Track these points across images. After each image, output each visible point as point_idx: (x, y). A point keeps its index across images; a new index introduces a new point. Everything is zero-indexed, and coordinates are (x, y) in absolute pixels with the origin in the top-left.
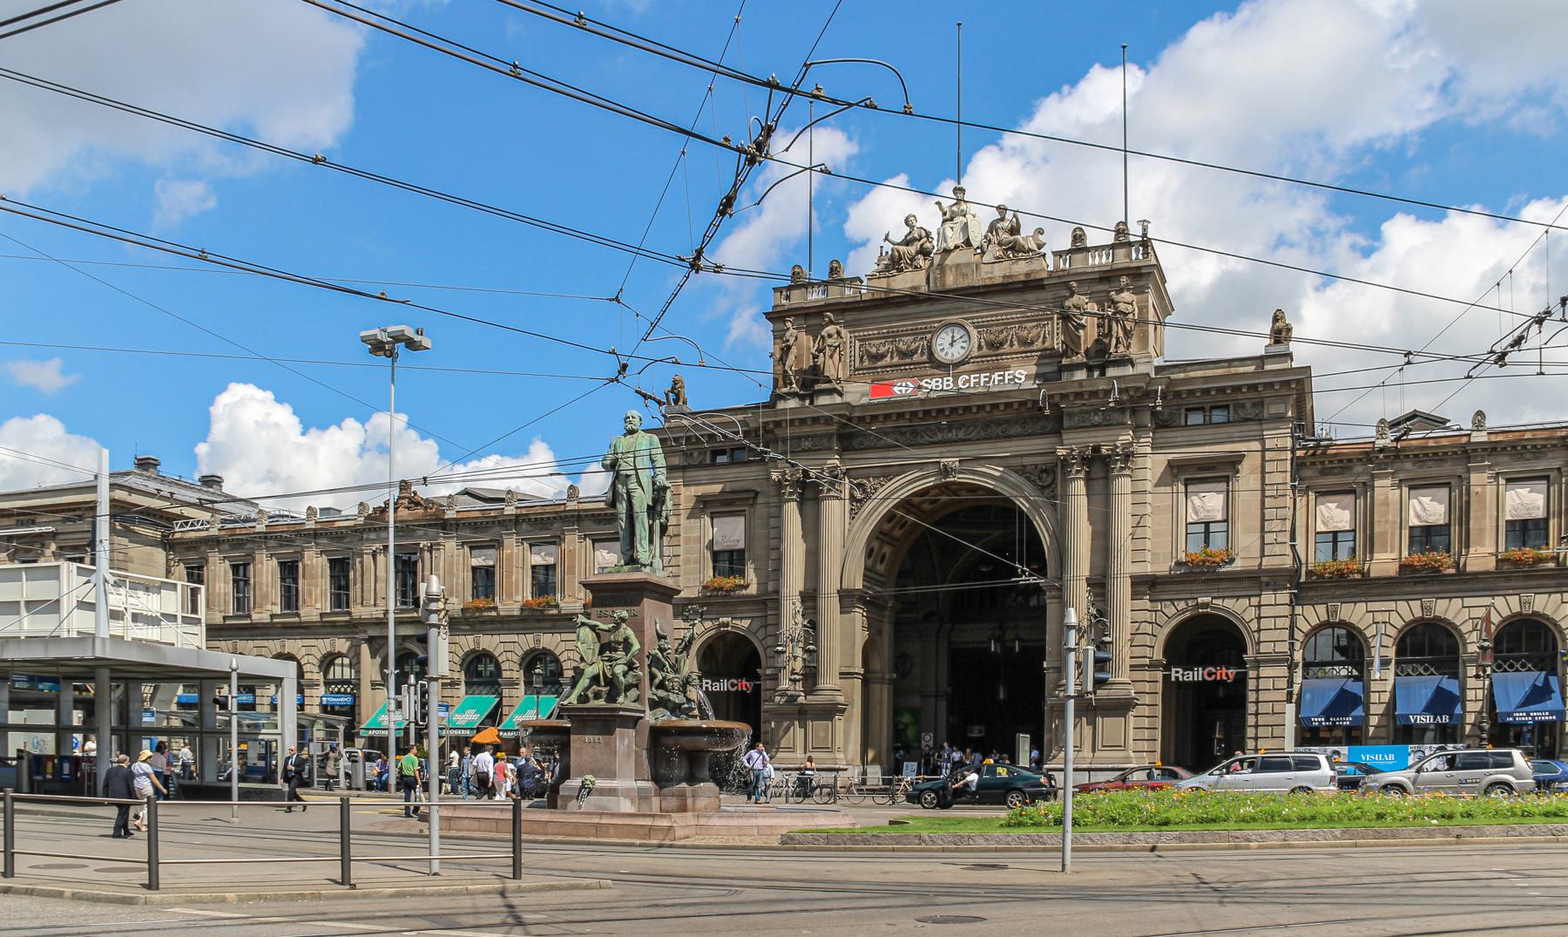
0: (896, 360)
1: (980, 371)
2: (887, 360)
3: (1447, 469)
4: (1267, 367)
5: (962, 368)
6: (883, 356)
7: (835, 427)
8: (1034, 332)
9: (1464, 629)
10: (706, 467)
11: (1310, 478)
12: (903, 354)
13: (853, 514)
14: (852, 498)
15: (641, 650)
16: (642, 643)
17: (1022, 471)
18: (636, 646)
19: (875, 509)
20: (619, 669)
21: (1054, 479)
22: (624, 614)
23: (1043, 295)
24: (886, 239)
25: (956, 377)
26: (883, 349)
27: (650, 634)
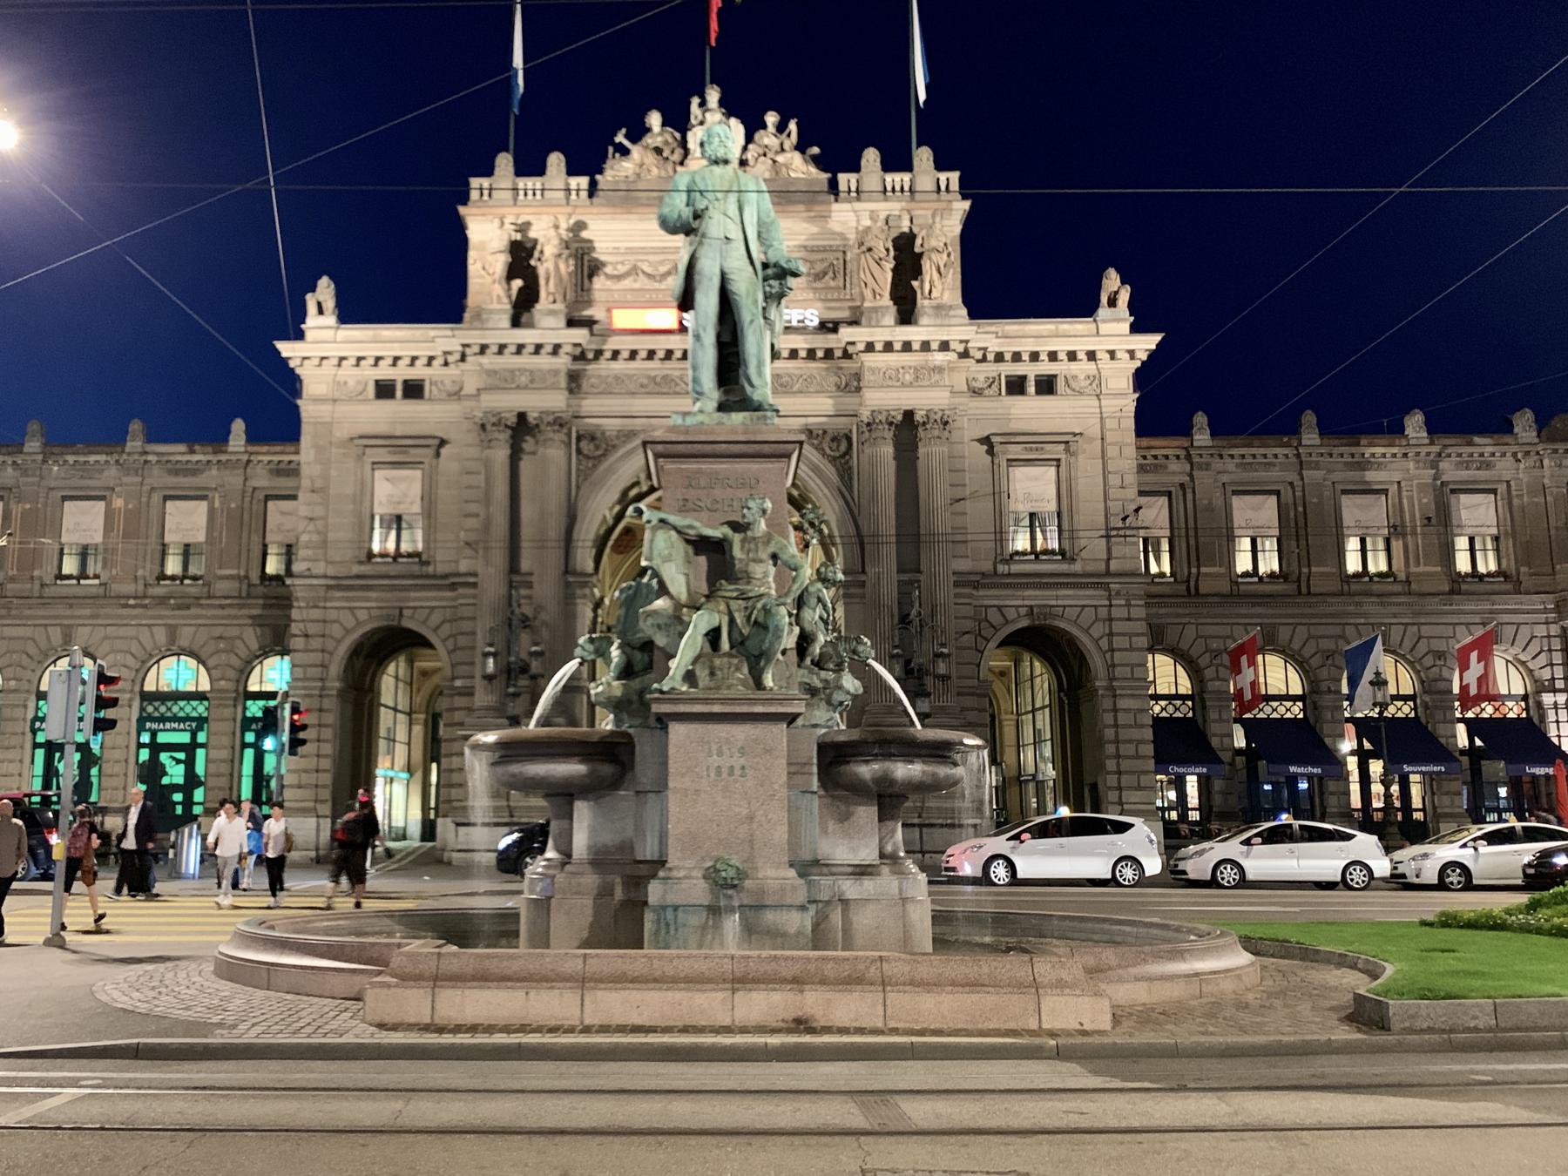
0: (637, 286)
12: (649, 276)
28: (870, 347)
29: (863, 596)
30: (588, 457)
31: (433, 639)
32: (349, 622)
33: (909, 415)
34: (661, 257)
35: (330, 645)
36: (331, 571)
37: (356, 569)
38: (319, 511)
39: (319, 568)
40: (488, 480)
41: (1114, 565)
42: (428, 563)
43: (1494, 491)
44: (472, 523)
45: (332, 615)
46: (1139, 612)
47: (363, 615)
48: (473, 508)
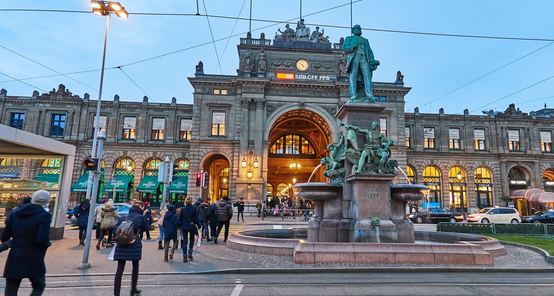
2: (280, 67)
3: (434, 123)
6: (279, 66)
8: (329, 66)
12: (286, 66)
14: (267, 110)
17: (325, 108)
23: (331, 55)
24: (279, 30)
26: (279, 64)
28: (342, 86)
30: (269, 111)
31: (227, 157)
32: (206, 152)
35: (200, 158)
36: (201, 139)
37: (208, 138)
38: (198, 122)
39: (198, 138)
40: (243, 116)
41: (399, 144)
43: (484, 129)
45: (201, 150)
46: (405, 155)
47: (209, 150)
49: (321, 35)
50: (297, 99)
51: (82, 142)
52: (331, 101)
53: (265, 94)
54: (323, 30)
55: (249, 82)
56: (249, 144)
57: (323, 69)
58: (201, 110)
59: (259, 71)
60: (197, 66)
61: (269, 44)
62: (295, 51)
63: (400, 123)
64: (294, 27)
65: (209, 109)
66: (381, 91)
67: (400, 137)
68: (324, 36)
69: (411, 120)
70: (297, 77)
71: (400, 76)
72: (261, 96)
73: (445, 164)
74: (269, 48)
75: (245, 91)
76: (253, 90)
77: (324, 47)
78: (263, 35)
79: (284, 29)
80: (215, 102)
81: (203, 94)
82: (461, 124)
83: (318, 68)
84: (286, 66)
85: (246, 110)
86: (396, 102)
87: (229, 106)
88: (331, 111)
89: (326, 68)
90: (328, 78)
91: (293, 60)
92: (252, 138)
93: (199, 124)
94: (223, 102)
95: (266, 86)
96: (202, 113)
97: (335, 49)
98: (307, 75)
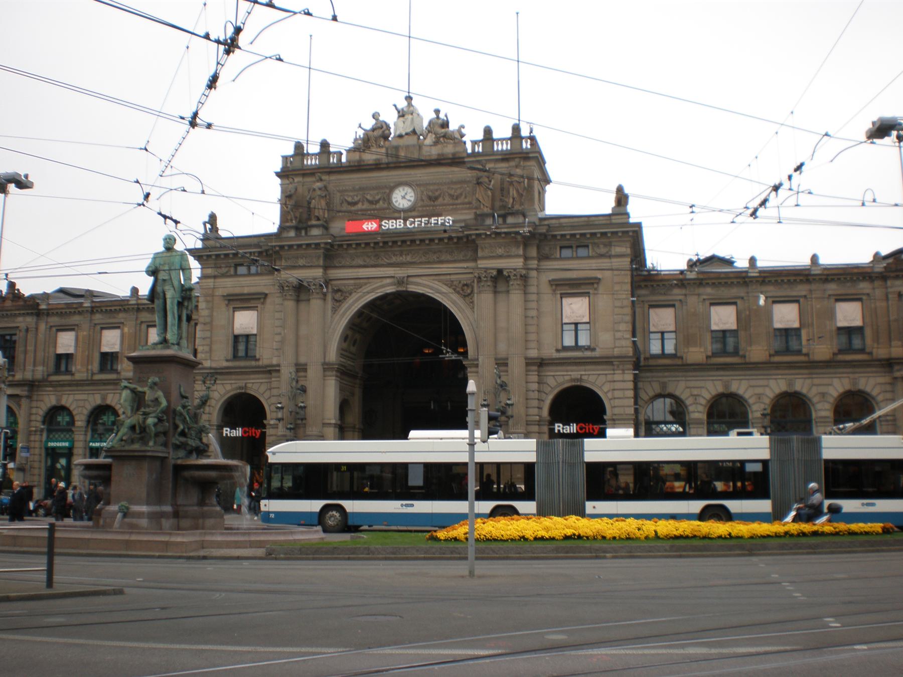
1: (422, 217)
2: (359, 206)
4: (614, 221)
5: (410, 214)
6: (355, 204)
7: (322, 251)
8: (459, 192)
9: (751, 401)
10: (231, 276)
11: (644, 296)
12: (371, 202)
13: (335, 310)
15: (168, 407)
16: (168, 401)
17: (450, 284)
18: (164, 403)
19: (349, 308)
20: (151, 421)
21: (472, 292)
22: (157, 379)
24: (360, 126)
25: (405, 220)
26: (356, 199)
27: (175, 395)
29: (477, 372)
33: (500, 271)
34: (375, 192)
42: (259, 360)
44: (278, 338)
48: (278, 330)
49: (445, 124)
50: (390, 271)
51: (39, 381)
52: (458, 269)
53: (326, 268)
54: (446, 116)
55: (291, 247)
56: (297, 371)
57: (447, 200)
58: (211, 309)
59: (314, 222)
60: (205, 224)
61: (340, 160)
62: (388, 167)
63: (618, 304)
64: (390, 117)
65: (227, 305)
66: (573, 235)
67: (618, 335)
68: (453, 127)
69: (676, 291)
70: (389, 225)
71: (622, 198)
72: (318, 273)
73: (759, 390)
74: (340, 169)
75: (289, 263)
76: (301, 262)
77: (449, 149)
78: (325, 145)
79: (369, 124)
80: (237, 291)
81: (215, 277)
82: (801, 290)
83: (436, 198)
84: (371, 202)
85: (290, 304)
86: (610, 257)
87: (262, 297)
88: (466, 291)
89: (451, 196)
90: (449, 220)
91: (386, 187)
92: (302, 360)
93: (211, 338)
94: (253, 290)
95: (327, 250)
96: (215, 314)
97: (474, 154)
98: (405, 220)
